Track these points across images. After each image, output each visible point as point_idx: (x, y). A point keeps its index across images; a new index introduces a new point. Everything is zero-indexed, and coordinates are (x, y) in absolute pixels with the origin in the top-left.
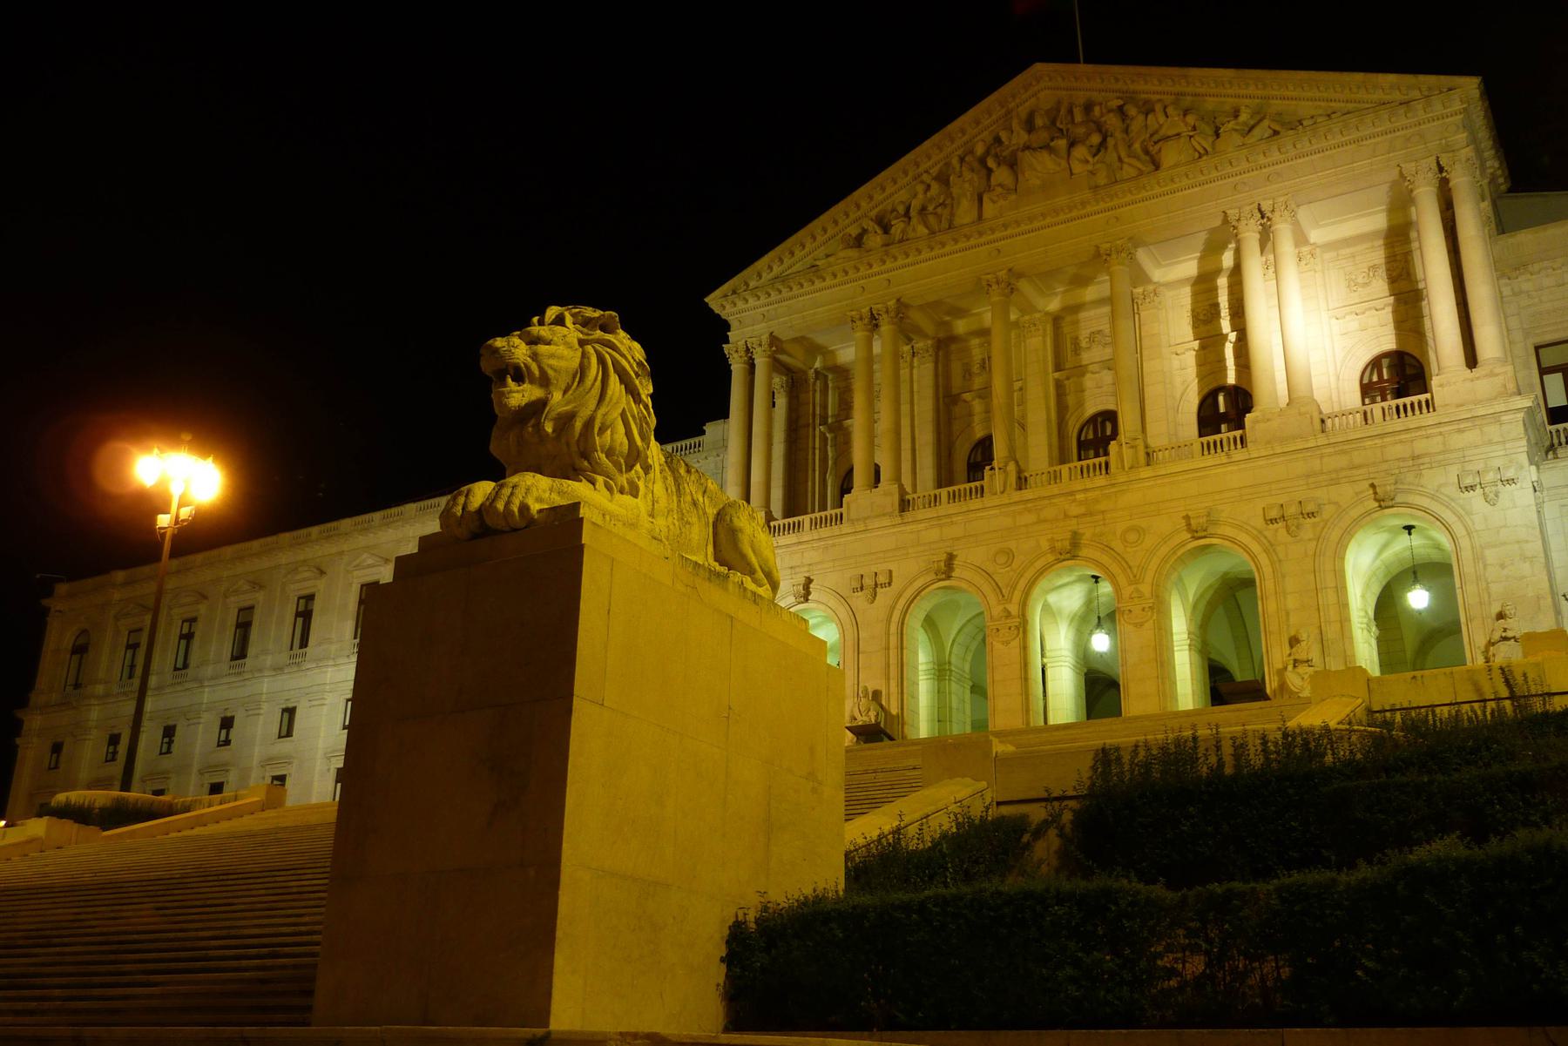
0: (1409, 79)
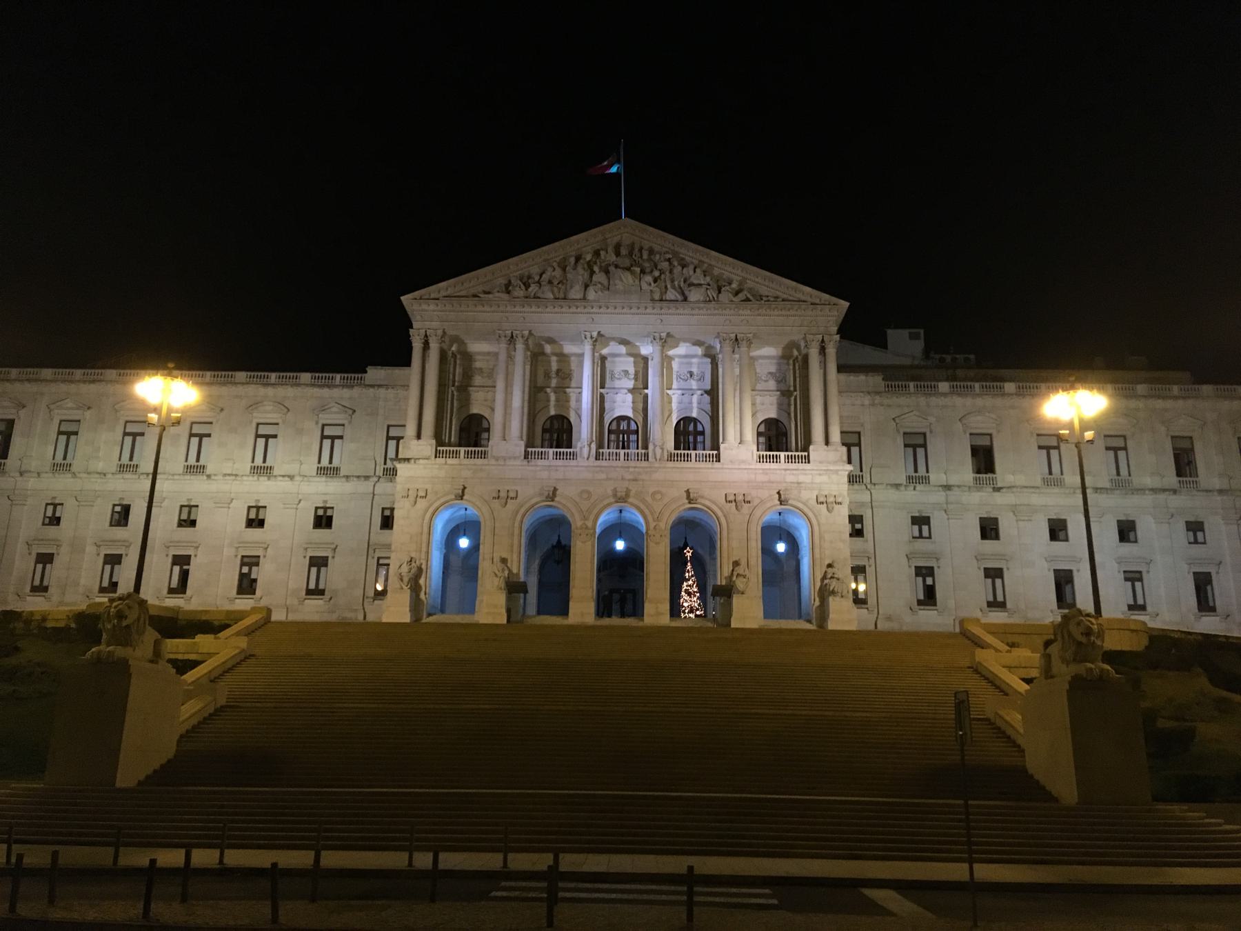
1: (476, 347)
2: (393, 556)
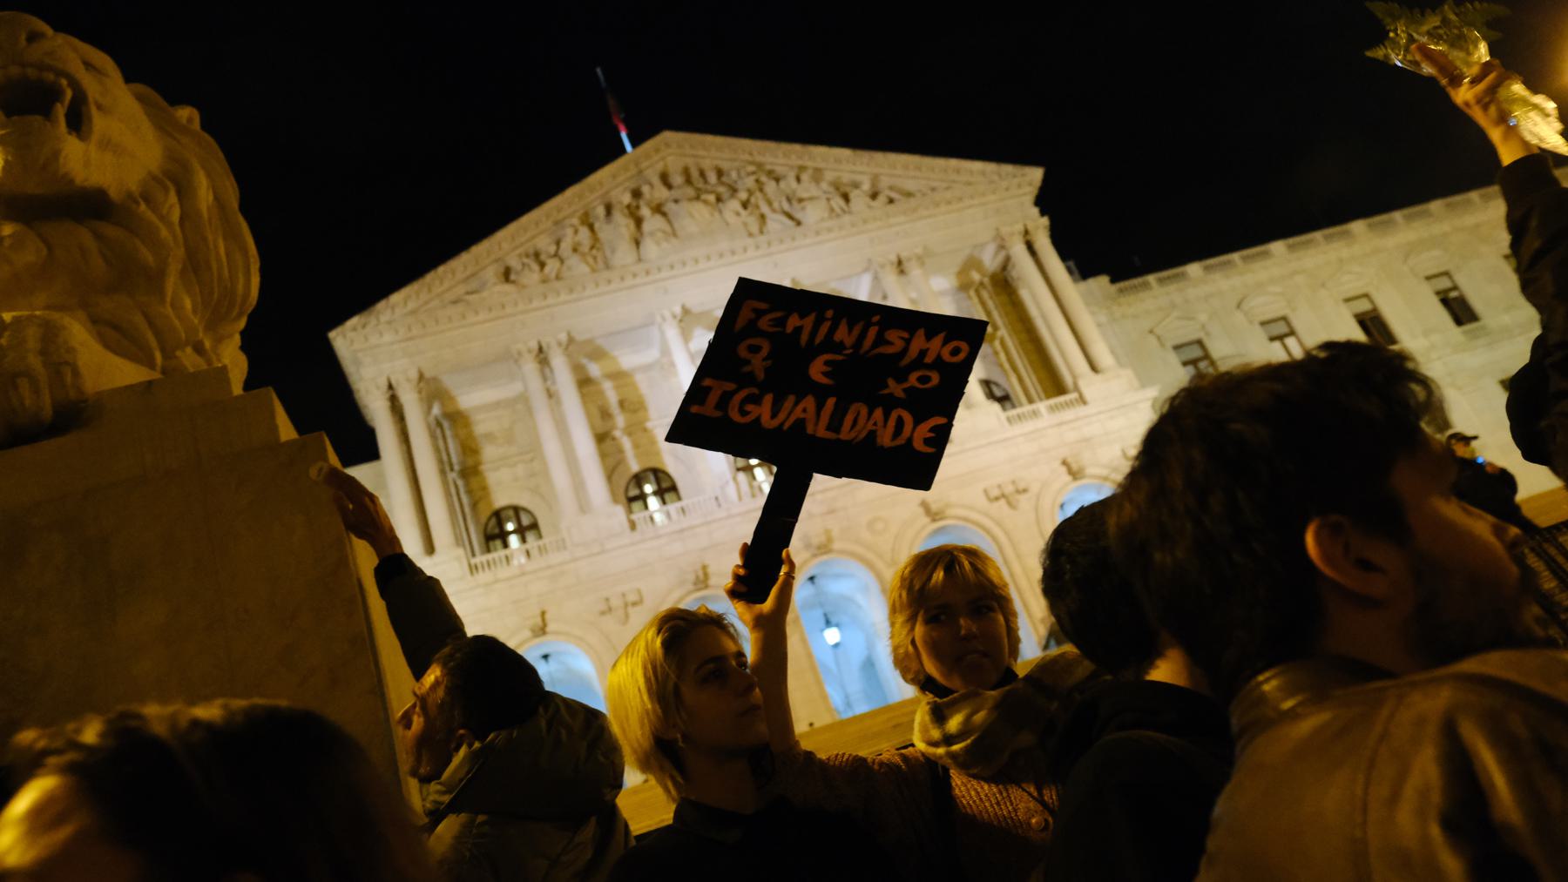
0: (990, 167)
1: (468, 400)
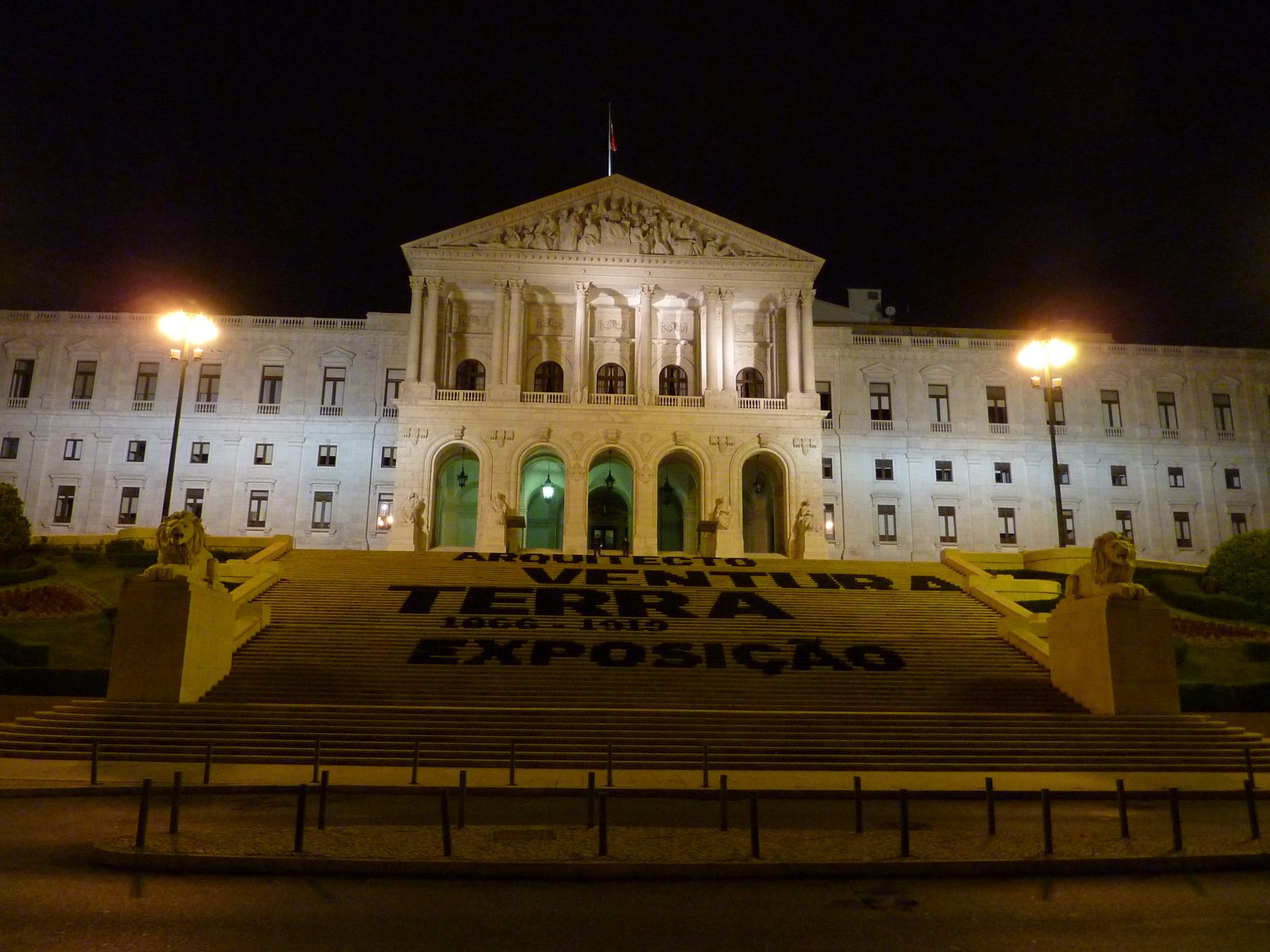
1: (471, 295)
2: (396, 492)
